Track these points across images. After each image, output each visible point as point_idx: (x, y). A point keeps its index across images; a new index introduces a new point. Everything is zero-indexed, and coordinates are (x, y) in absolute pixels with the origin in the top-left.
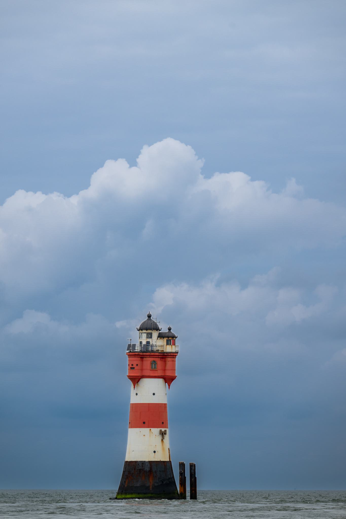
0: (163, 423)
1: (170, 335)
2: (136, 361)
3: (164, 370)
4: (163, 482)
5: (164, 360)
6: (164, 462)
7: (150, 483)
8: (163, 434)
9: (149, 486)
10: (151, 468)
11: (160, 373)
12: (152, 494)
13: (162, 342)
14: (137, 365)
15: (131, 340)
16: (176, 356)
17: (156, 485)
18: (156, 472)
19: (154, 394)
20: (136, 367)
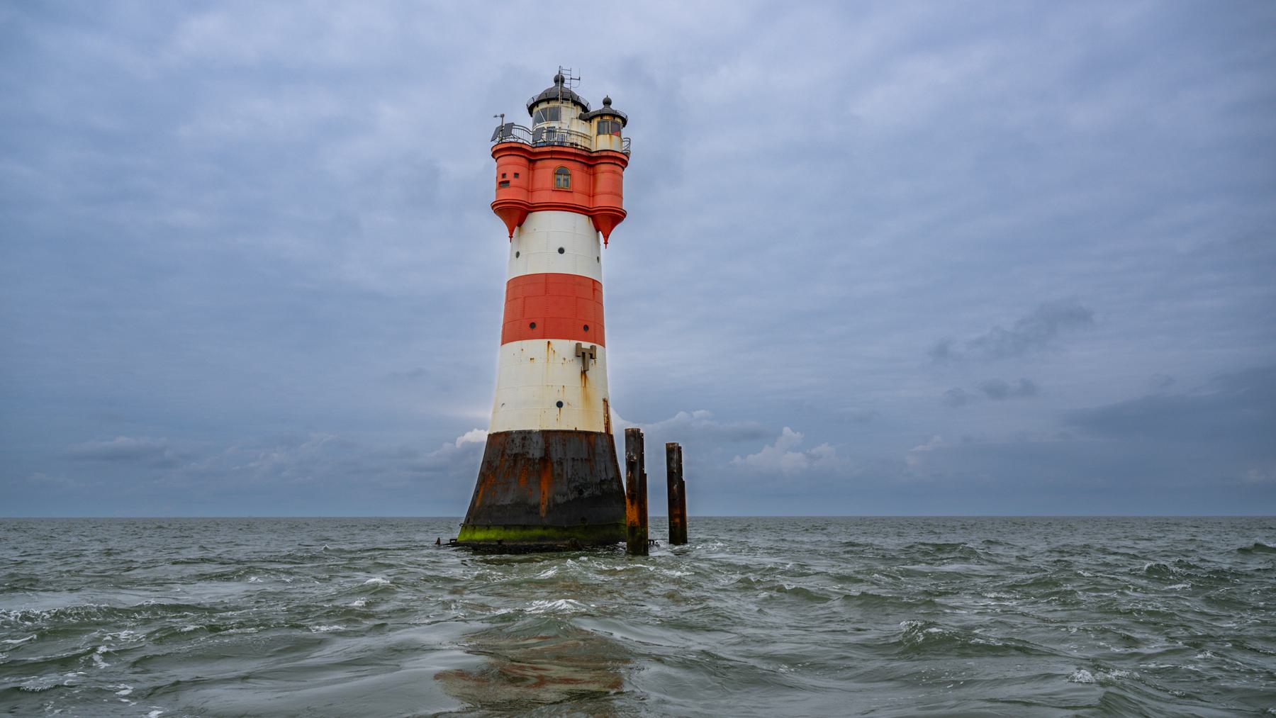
0: (586, 328)
2: (515, 164)
3: (592, 195)
4: (581, 492)
6: (588, 434)
7: (542, 494)
8: (585, 357)
9: (537, 506)
10: (547, 451)
12: (545, 528)
13: (591, 129)
14: (516, 175)
15: (502, 116)
17: (560, 499)
18: (560, 463)
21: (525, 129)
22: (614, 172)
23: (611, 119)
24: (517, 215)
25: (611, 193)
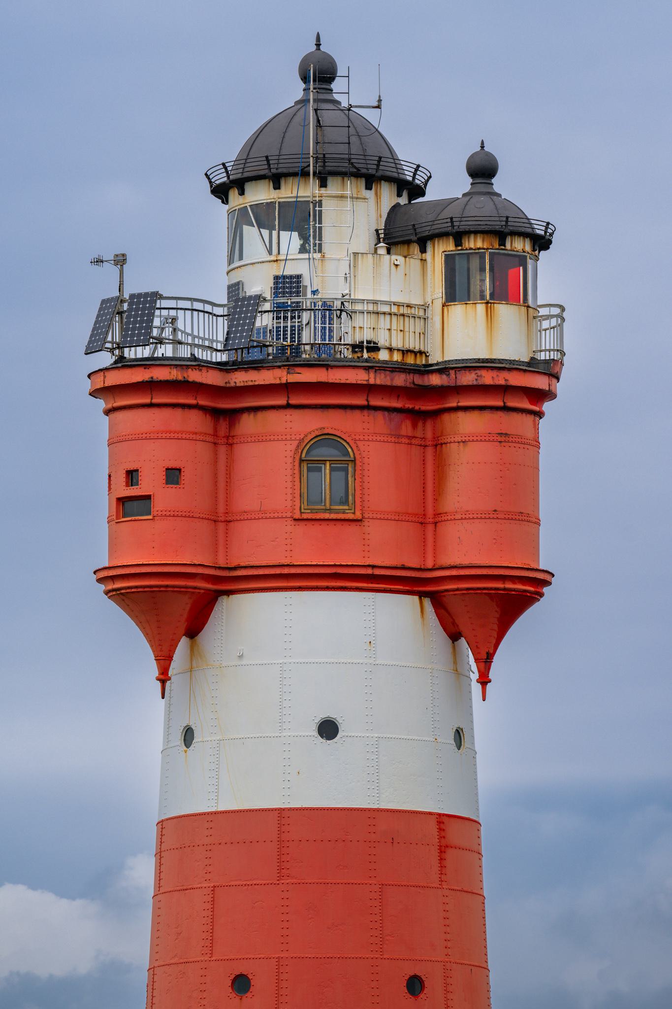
1: (482, 209)
2: (169, 438)
3: (427, 519)
5: (427, 430)
11: (382, 544)
13: (413, 280)
14: (173, 475)
15: (121, 261)
16: (541, 396)
19: (328, 729)
20: (165, 498)
21: (204, 273)
22: (504, 438)
23: (486, 241)
24: (182, 607)
25: (494, 515)
